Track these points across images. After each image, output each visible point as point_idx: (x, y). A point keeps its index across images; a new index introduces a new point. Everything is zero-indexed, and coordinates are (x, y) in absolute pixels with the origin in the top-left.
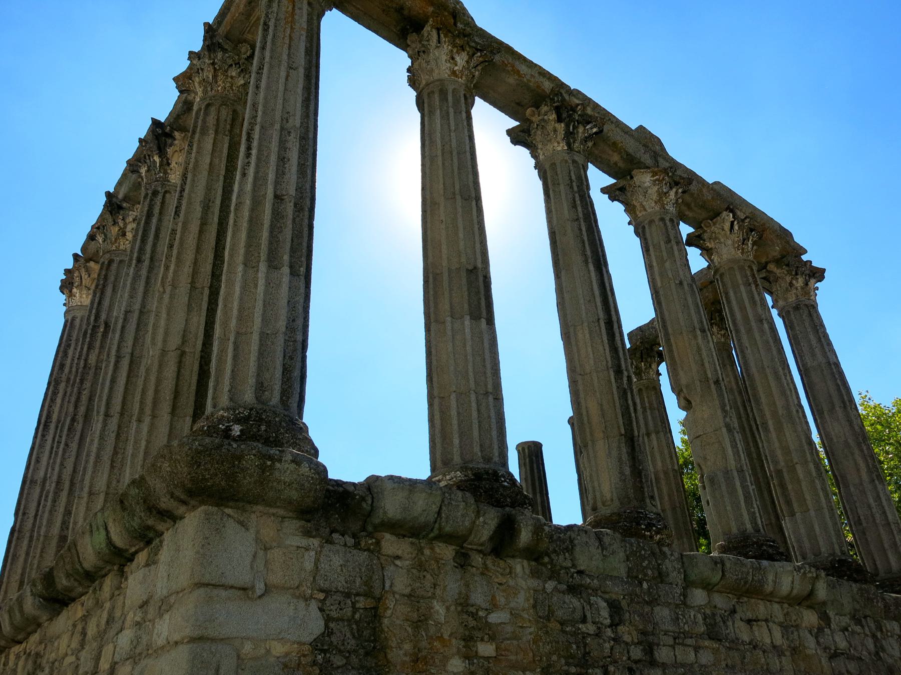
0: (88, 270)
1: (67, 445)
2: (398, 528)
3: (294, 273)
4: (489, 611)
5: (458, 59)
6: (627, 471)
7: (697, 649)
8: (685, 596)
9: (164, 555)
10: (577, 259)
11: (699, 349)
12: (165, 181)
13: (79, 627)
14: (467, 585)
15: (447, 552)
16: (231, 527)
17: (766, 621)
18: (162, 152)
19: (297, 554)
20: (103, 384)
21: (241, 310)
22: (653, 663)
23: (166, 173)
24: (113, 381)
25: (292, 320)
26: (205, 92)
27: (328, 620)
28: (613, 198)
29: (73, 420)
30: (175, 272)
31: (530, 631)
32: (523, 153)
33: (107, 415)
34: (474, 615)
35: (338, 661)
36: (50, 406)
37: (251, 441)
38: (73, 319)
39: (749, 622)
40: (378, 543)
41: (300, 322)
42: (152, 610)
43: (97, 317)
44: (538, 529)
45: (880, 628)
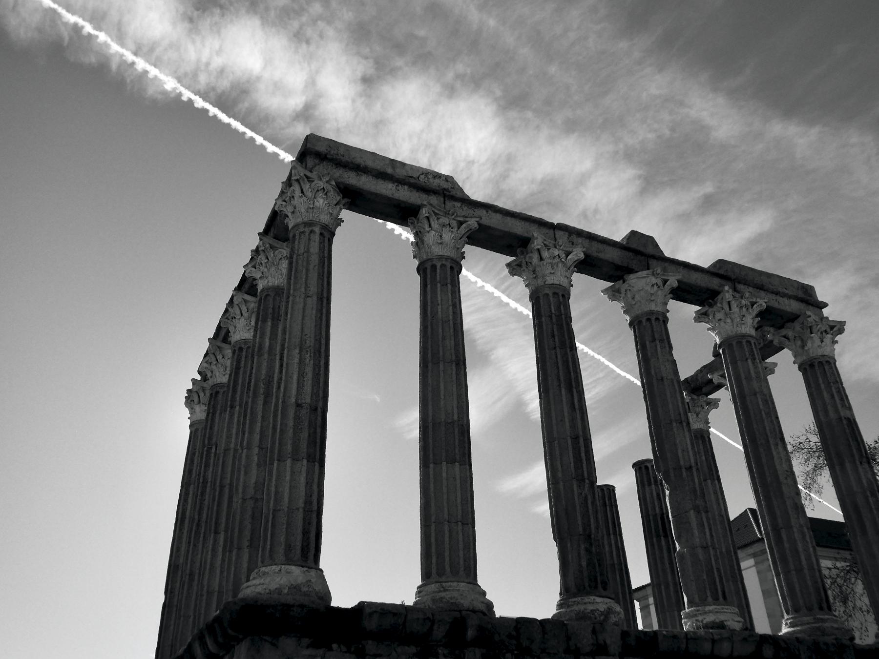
1: (195, 545)
6: (584, 564)
25: (308, 502)
36: (184, 505)
38: (197, 430)
43: (210, 439)
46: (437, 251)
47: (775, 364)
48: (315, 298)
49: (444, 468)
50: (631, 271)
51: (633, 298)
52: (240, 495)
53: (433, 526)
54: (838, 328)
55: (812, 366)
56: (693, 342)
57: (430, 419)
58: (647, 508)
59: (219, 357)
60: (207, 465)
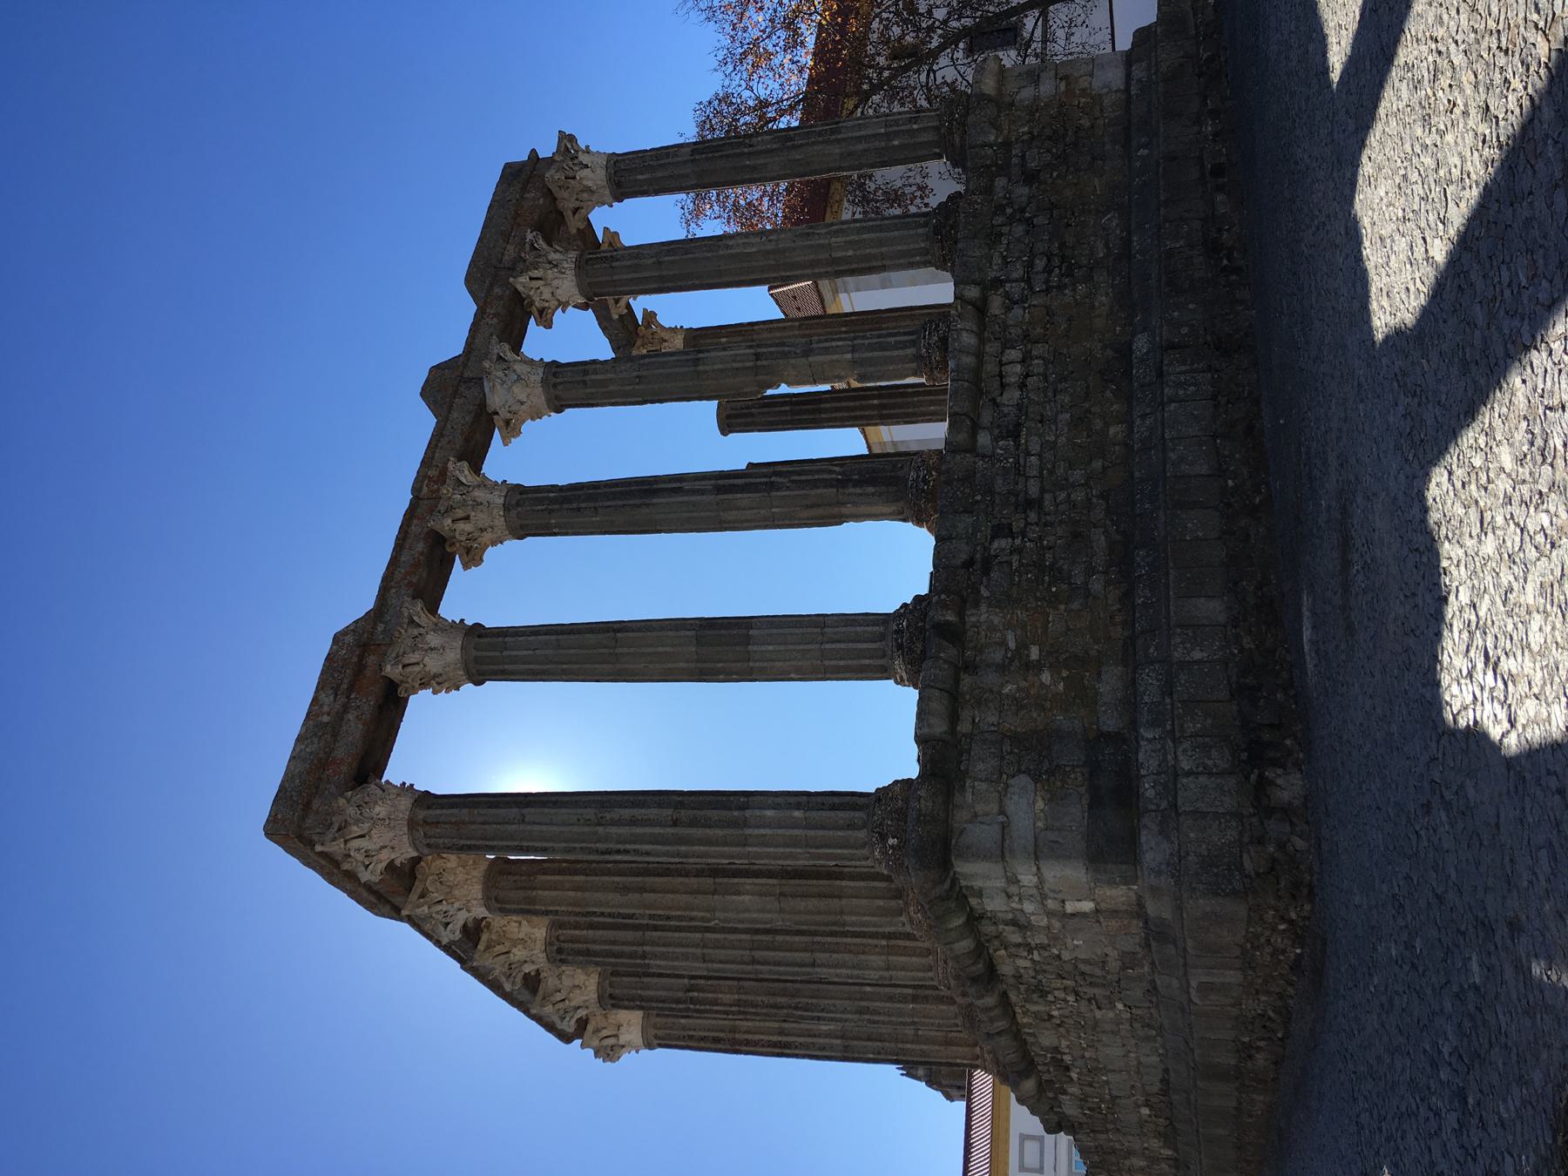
2: (954, 718)
3: (743, 808)
4: (1007, 649)
6: (871, 489)
7: (1029, 454)
8: (984, 456)
9: (977, 884)
13: (1013, 950)
14: (988, 666)
15: (967, 681)
17: (1001, 364)
19: (977, 798)
22: (1041, 500)
24: (778, 964)
27: (1019, 771)
29: (796, 1008)
33: (813, 965)
34: (1012, 660)
37: (909, 828)
38: (656, 1037)
39: (1003, 386)
41: (792, 800)
42: (1013, 889)
44: (944, 605)
45: (1000, 209)
46: (453, 655)
47: (606, 229)
48: (525, 811)
49: (755, 648)
50: (483, 404)
51: (522, 403)
52: (775, 916)
53: (827, 663)
54: (567, 140)
55: (619, 185)
56: (574, 336)
57: (693, 665)
58: (787, 422)
59: (559, 996)
60: (715, 1002)
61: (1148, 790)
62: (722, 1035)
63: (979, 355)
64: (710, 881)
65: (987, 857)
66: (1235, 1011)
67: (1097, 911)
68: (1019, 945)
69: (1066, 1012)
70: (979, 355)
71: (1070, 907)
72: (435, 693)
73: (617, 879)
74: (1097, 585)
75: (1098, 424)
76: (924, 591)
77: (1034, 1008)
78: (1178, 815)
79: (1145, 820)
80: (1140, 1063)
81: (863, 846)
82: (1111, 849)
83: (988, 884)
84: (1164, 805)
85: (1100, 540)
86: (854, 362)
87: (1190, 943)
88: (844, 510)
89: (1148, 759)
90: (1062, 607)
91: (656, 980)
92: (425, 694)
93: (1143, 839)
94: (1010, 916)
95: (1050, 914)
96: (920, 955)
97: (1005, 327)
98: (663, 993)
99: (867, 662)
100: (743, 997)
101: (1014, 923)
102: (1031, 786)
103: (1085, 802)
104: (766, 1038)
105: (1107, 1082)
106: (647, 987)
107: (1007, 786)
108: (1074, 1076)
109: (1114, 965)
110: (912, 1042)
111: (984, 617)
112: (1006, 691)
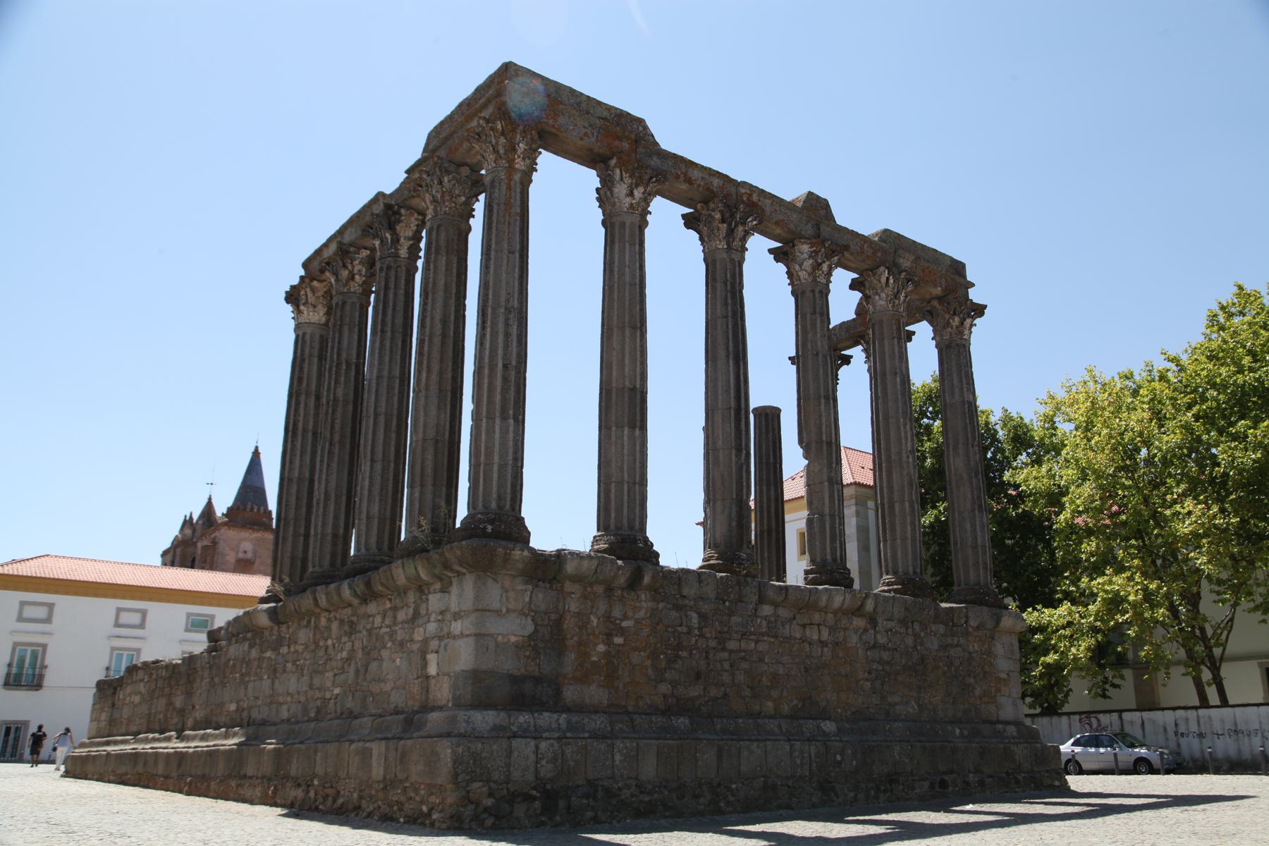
0: (313, 290)
4: (622, 620)
5: (636, 192)
6: (734, 524)
7: (756, 643)
9: (455, 590)
10: (722, 353)
11: (820, 416)
12: (397, 256)
15: (599, 589)
16: (490, 582)
17: (819, 625)
18: (391, 227)
19: (522, 593)
20: (366, 434)
21: (486, 449)
22: (724, 649)
23: (396, 249)
26: (435, 210)
27: (536, 625)
28: (777, 260)
29: (331, 444)
30: (427, 378)
31: (646, 631)
32: (693, 236)
33: (373, 461)
35: (541, 645)
40: (562, 587)
42: (448, 616)
49: (626, 432)
60: (337, 382)
61: (524, 718)
62: (304, 384)
63: (824, 610)
64: (449, 388)
65: (477, 598)
66: (342, 774)
67: (428, 677)
68: (395, 617)
69: (330, 650)
70: (824, 610)
71: (432, 658)
72: (597, 190)
73: (452, 318)
74: (664, 688)
75: (775, 694)
76: (663, 561)
77: (335, 626)
78: (509, 738)
79: (503, 714)
80: (282, 704)
81: (484, 506)
82: (482, 690)
83: (454, 598)
84: (514, 728)
85: (695, 691)
86: (822, 515)
87: (409, 742)
88: (719, 504)
89: (546, 719)
90: (649, 663)
91: (356, 337)
92: (597, 183)
93: (491, 712)
94: (423, 612)
95: (425, 642)
96: (378, 542)
97: (845, 629)
98: (345, 343)
99: (613, 515)
100: (341, 404)
101: (416, 615)
102: (527, 633)
103: (516, 672)
104: (301, 419)
105: (261, 679)
106: (351, 331)
107: (526, 616)
108: (268, 654)
109: (375, 688)
110: (295, 531)
111: (644, 604)
112: (592, 618)
